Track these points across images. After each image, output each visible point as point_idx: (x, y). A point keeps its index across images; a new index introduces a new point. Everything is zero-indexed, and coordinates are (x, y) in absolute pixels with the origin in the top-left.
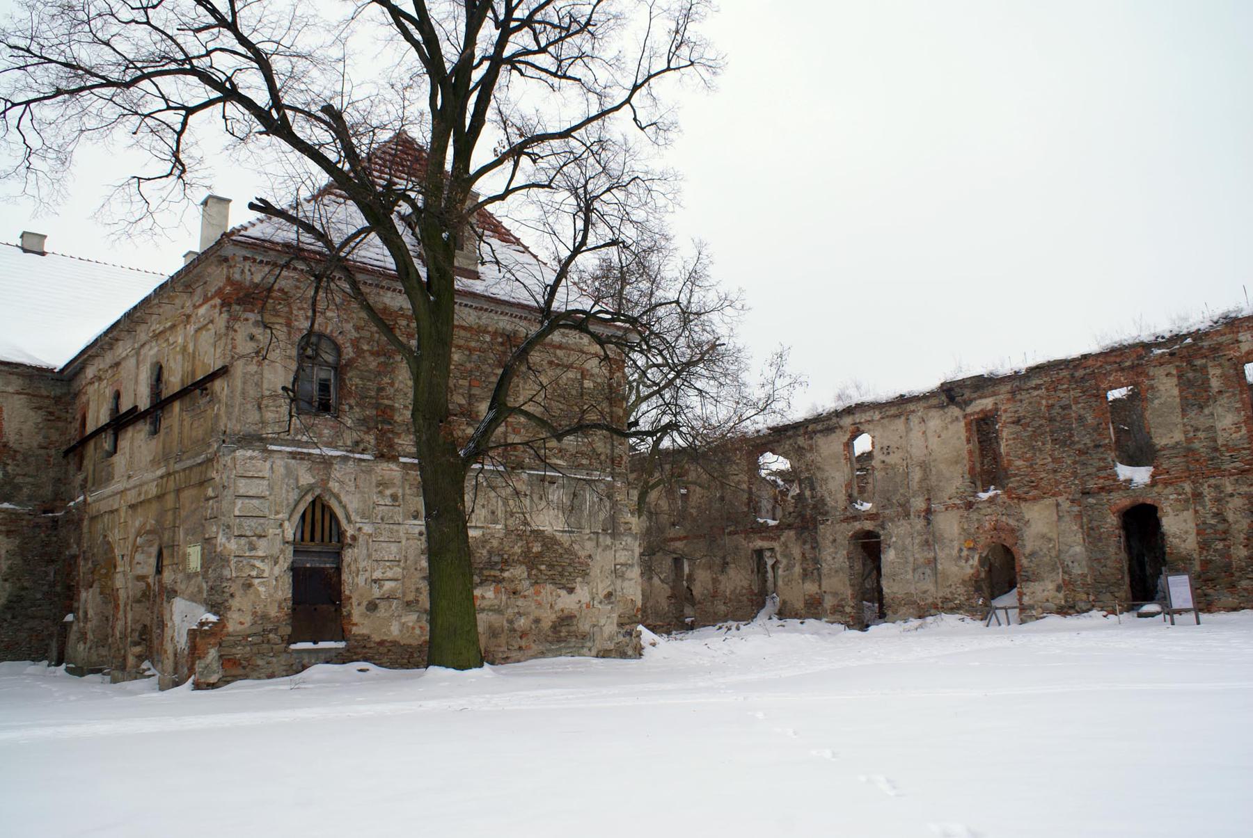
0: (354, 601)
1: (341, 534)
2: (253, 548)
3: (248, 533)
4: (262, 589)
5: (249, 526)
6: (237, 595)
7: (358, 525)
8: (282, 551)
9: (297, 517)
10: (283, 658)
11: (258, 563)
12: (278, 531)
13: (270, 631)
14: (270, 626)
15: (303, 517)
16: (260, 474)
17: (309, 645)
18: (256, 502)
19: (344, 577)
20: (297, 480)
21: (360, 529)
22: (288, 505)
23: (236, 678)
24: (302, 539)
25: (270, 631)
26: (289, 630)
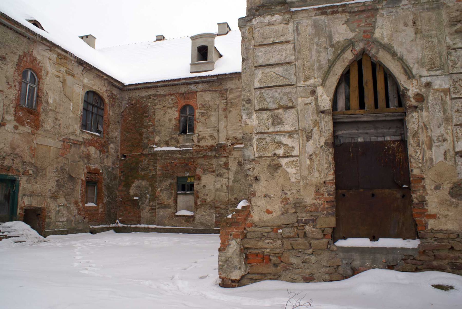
0: (429, 184)
1: (401, 97)
2: (277, 121)
3: (272, 106)
4: (291, 171)
5: (272, 98)
6: (262, 178)
7: (424, 80)
8: (316, 123)
9: (333, 80)
10: (325, 257)
11: (285, 140)
12: (310, 99)
13: (306, 223)
14: (305, 216)
15: (345, 77)
16: (283, 39)
17: (364, 242)
18: (279, 70)
19: (411, 151)
20: (330, 37)
21: (428, 85)
22: (320, 68)
23: (264, 277)
24: (348, 108)
25: (306, 223)
26: (332, 221)
